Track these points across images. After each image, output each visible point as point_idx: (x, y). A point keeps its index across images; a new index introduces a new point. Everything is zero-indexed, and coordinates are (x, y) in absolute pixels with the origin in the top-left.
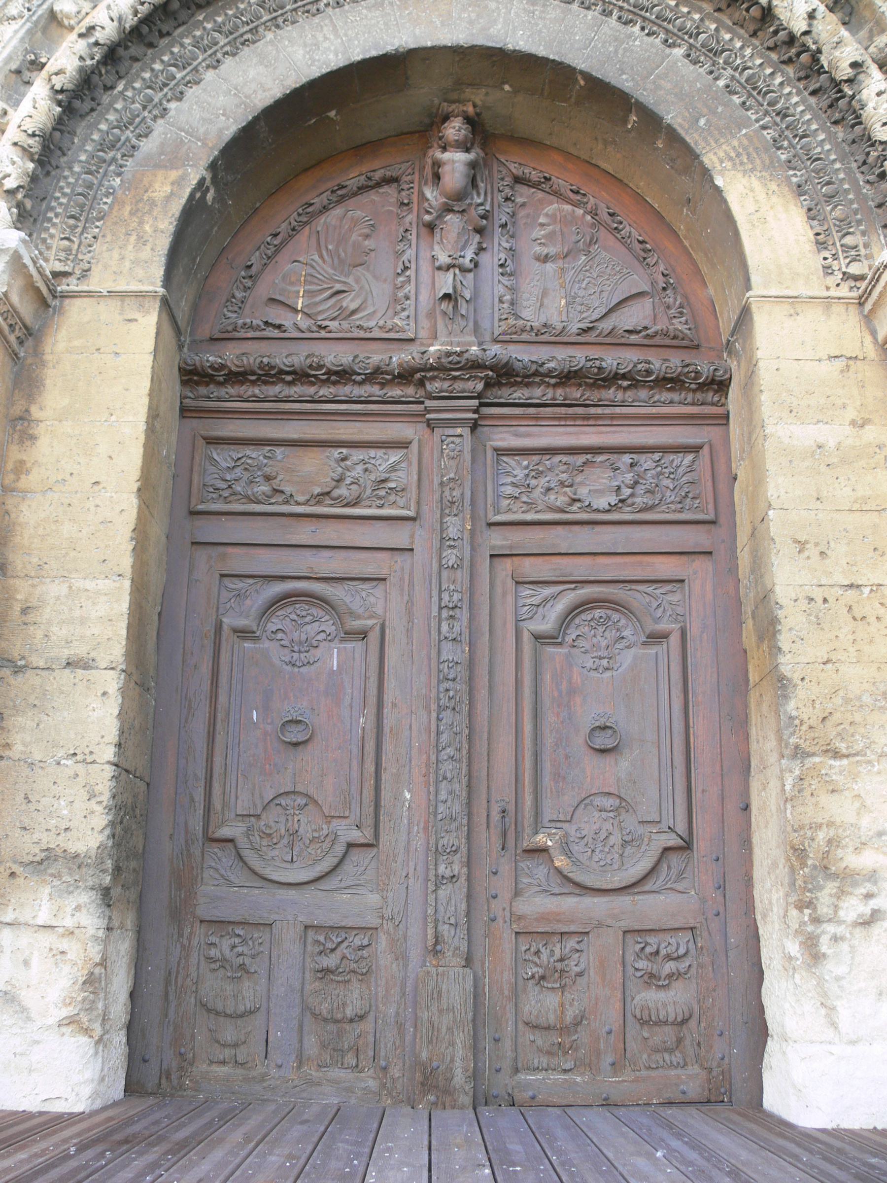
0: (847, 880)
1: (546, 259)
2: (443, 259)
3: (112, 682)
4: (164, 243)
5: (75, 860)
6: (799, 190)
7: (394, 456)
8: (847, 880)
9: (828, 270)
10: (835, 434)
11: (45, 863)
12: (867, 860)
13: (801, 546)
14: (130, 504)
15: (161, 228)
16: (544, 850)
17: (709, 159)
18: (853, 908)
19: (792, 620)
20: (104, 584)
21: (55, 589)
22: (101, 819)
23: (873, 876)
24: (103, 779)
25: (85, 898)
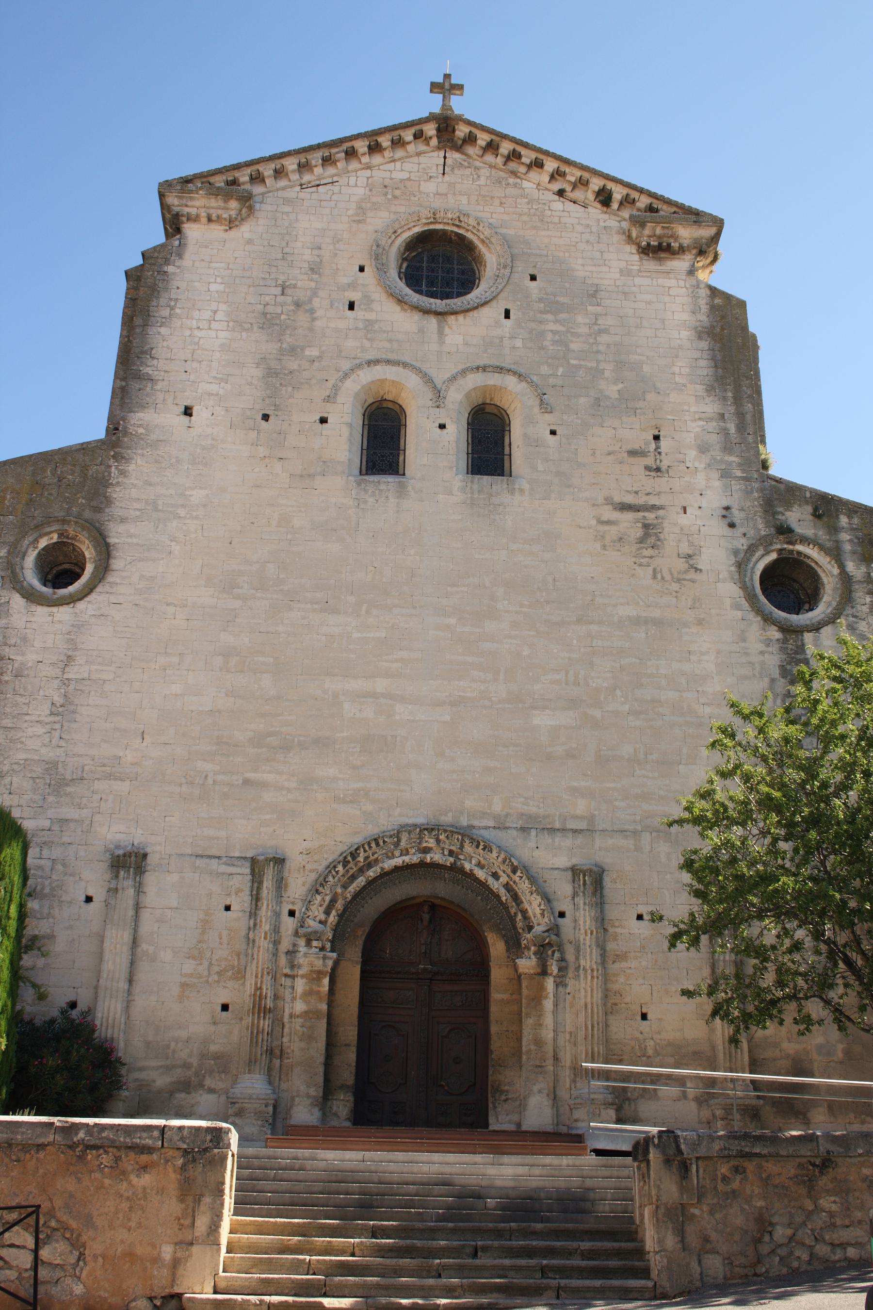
0: (502, 1092)
1: (447, 940)
2: (423, 942)
3: (354, 1049)
4: (361, 947)
5: (348, 1086)
6: (504, 936)
7: (411, 992)
8: (502, 1092)
9: (508, 957)
10: (505, 996)
11: (343, 1087)
12: (506, 1088)
13: (497, 1022)
14: (357, 1010)
15: (360, 943)
16: (442, 1086)
17: (484, 928)
18: (503, 1097)
19: (494, 1038)
20: (352, 1028)
21: (342, 1029)
22: (353, 1078)
23: (507, 1091)
24: (353, 1070)
25: (350, 1094)
